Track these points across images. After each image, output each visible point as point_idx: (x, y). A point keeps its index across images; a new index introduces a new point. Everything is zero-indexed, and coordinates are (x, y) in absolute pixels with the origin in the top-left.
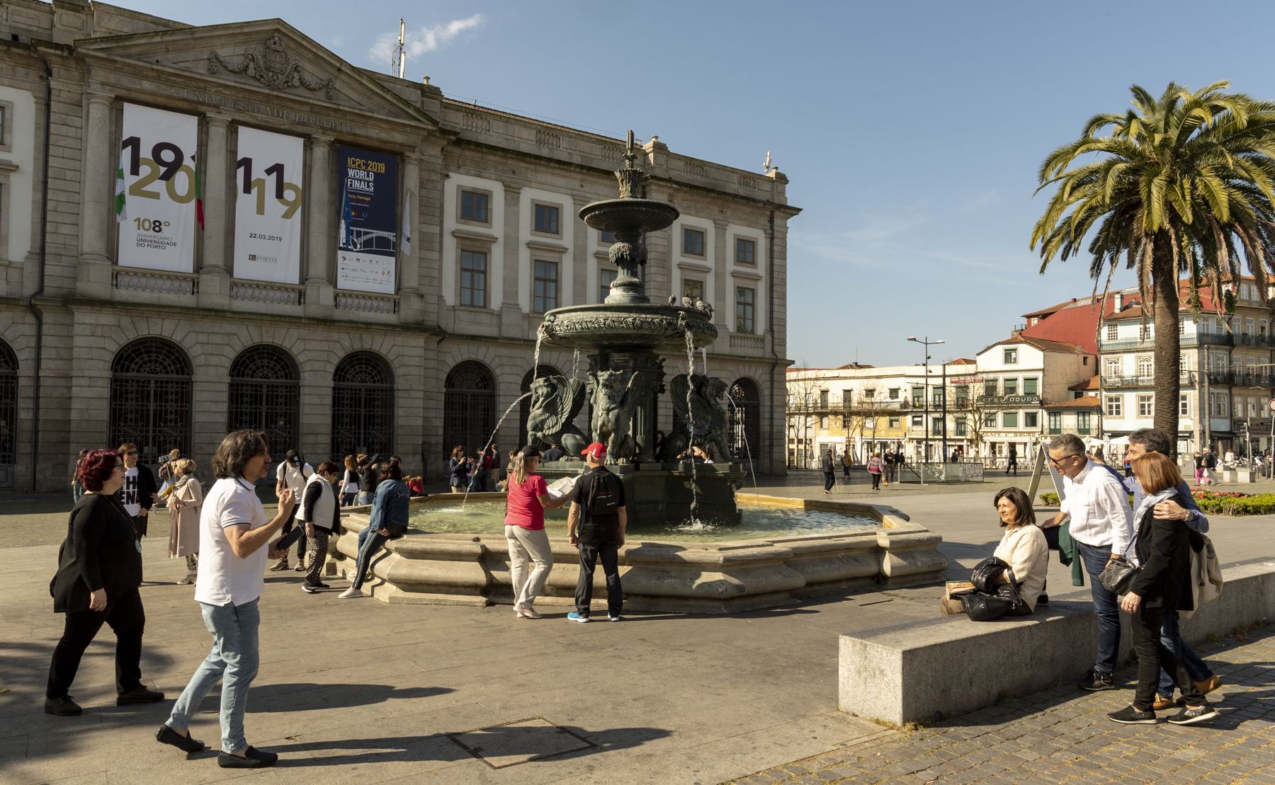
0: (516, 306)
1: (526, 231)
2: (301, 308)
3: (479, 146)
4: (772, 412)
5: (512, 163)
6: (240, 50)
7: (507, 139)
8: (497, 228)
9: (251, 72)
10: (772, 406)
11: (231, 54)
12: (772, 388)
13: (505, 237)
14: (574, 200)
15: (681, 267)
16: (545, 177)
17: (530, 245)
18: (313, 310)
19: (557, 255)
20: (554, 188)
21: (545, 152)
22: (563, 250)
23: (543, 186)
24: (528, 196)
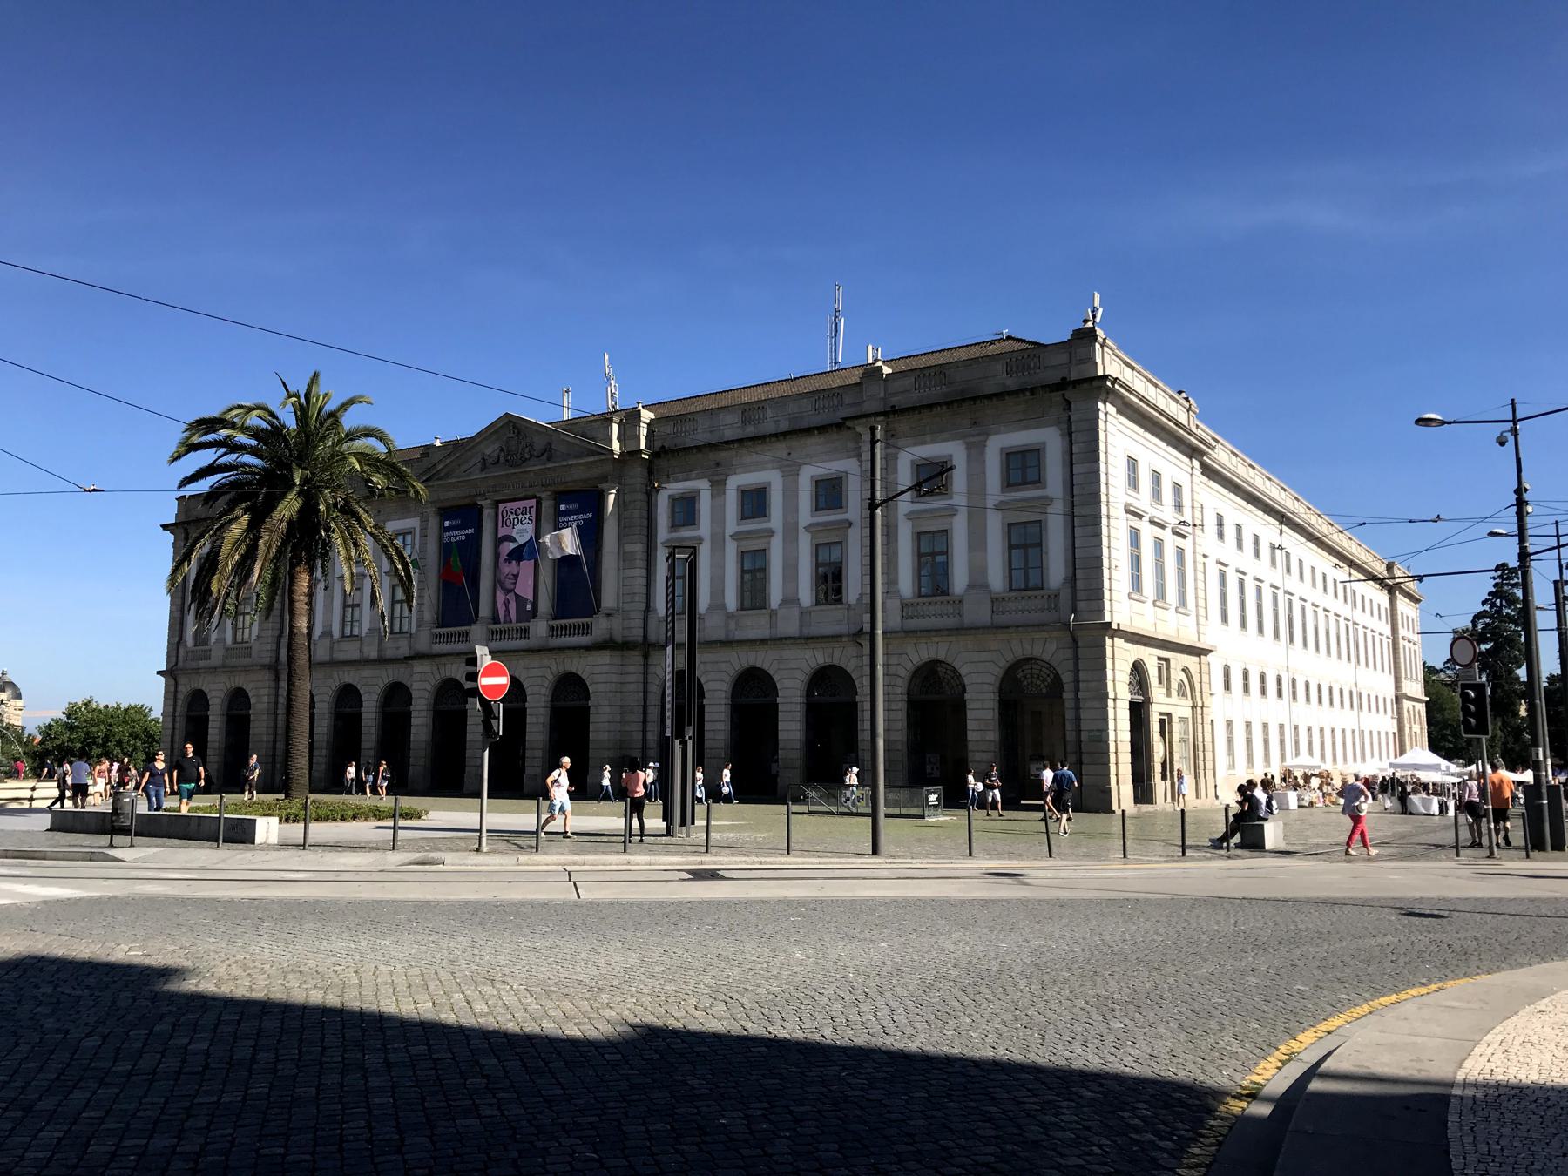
0: (723, 606)
1: (732, 524)
2: (527, 641)
3: (686, 450)
4: (1077, 708)
5: (714, 456)
6: (497, 446)
7: (711, 432)
8: (704, 527)
9: (502, 460)
10: (1077, 699)
11: (491, 450)
12: (1076, 671)
13: (712, 535)
14: (782, 472)
15: (910, 516)
16: (748, 456)
17: (735, 536)
18: (533, 642)
19: (764, 540)
20: (760, 467)
21: (750, 431)
22: (771, 533)
23: (748, 468)
24: (735, 482)
